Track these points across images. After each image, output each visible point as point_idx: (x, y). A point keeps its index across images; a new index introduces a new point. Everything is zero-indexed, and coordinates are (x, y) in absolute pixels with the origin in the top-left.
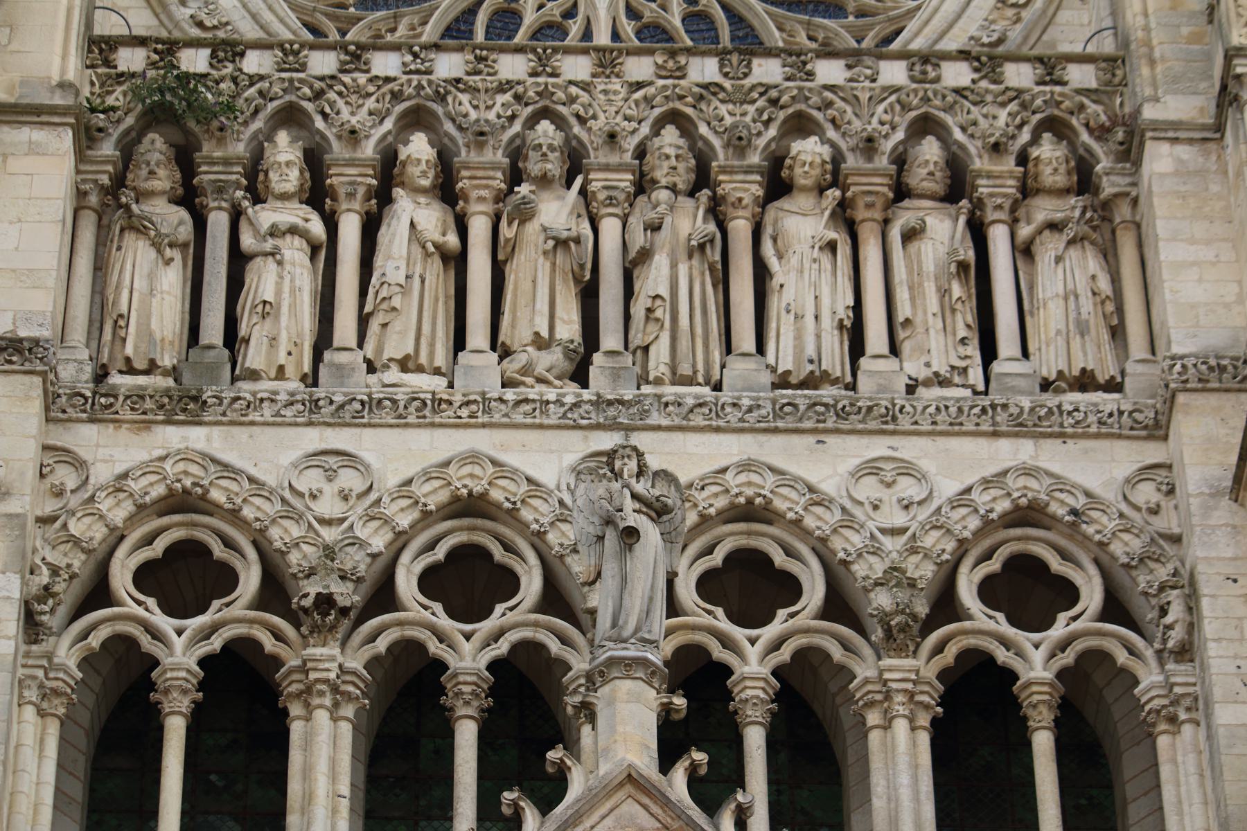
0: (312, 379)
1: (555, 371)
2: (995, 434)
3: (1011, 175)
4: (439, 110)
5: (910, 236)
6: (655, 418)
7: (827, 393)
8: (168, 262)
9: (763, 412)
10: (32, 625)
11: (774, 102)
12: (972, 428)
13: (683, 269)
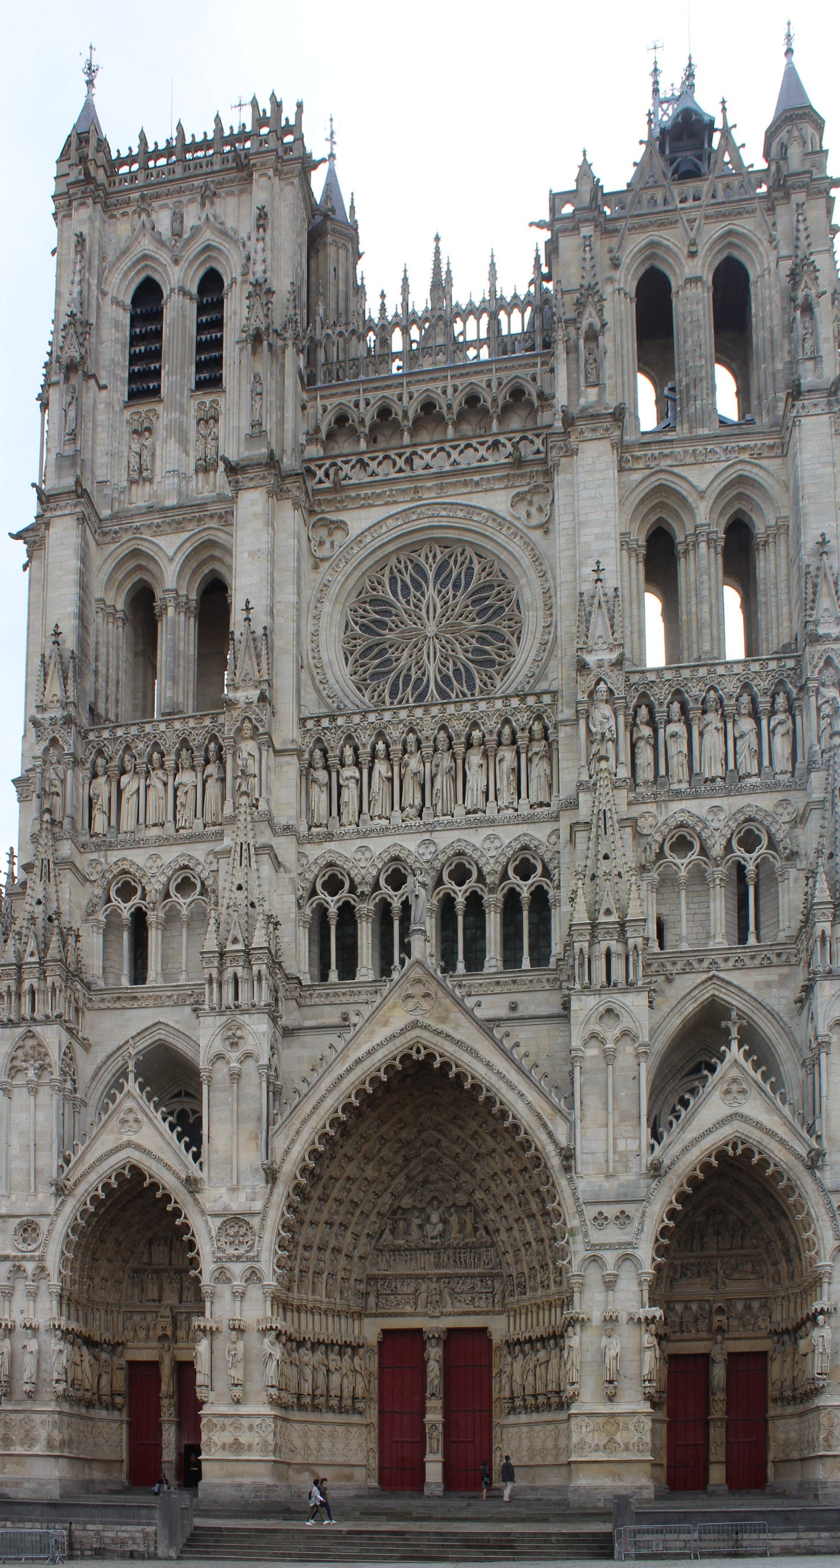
5: (500, 761)
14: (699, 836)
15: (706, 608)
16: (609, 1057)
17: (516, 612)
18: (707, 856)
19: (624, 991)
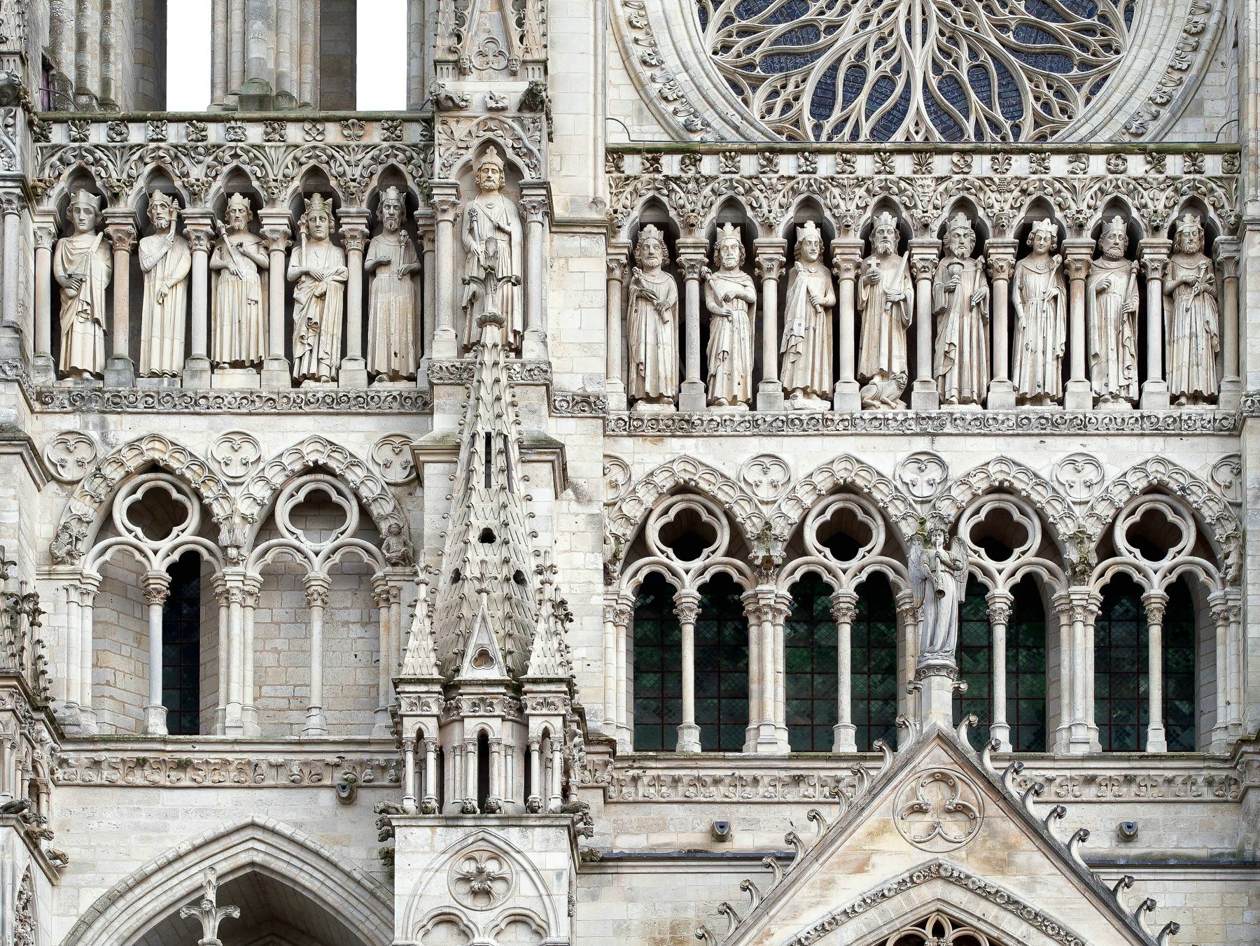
0: (753, 406)
1: (892, 397)
2: (1142, 435)
4: (822, 202)
5: (1100, 292)
6: (948, 429)
7: (1049, 408)
8: (665, 323)
10: (608, 578)
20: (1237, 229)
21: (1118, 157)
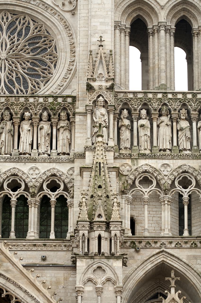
2: (50, 162)
3: (57, 118)
5: (41, 129)
7: (27, 155)
9: (17, 159)
11: (22, 105)
12: (47, 162)
13: (7, 135)
14: (156, 178)
15: (163, 62)
16: (99, 291)
17: (54, 52)
18: (160, 188)
19: (108, 258)
20: (74, 114)
21: (46, 98)
